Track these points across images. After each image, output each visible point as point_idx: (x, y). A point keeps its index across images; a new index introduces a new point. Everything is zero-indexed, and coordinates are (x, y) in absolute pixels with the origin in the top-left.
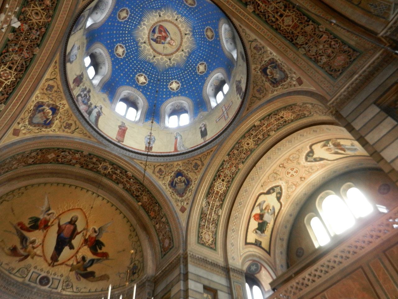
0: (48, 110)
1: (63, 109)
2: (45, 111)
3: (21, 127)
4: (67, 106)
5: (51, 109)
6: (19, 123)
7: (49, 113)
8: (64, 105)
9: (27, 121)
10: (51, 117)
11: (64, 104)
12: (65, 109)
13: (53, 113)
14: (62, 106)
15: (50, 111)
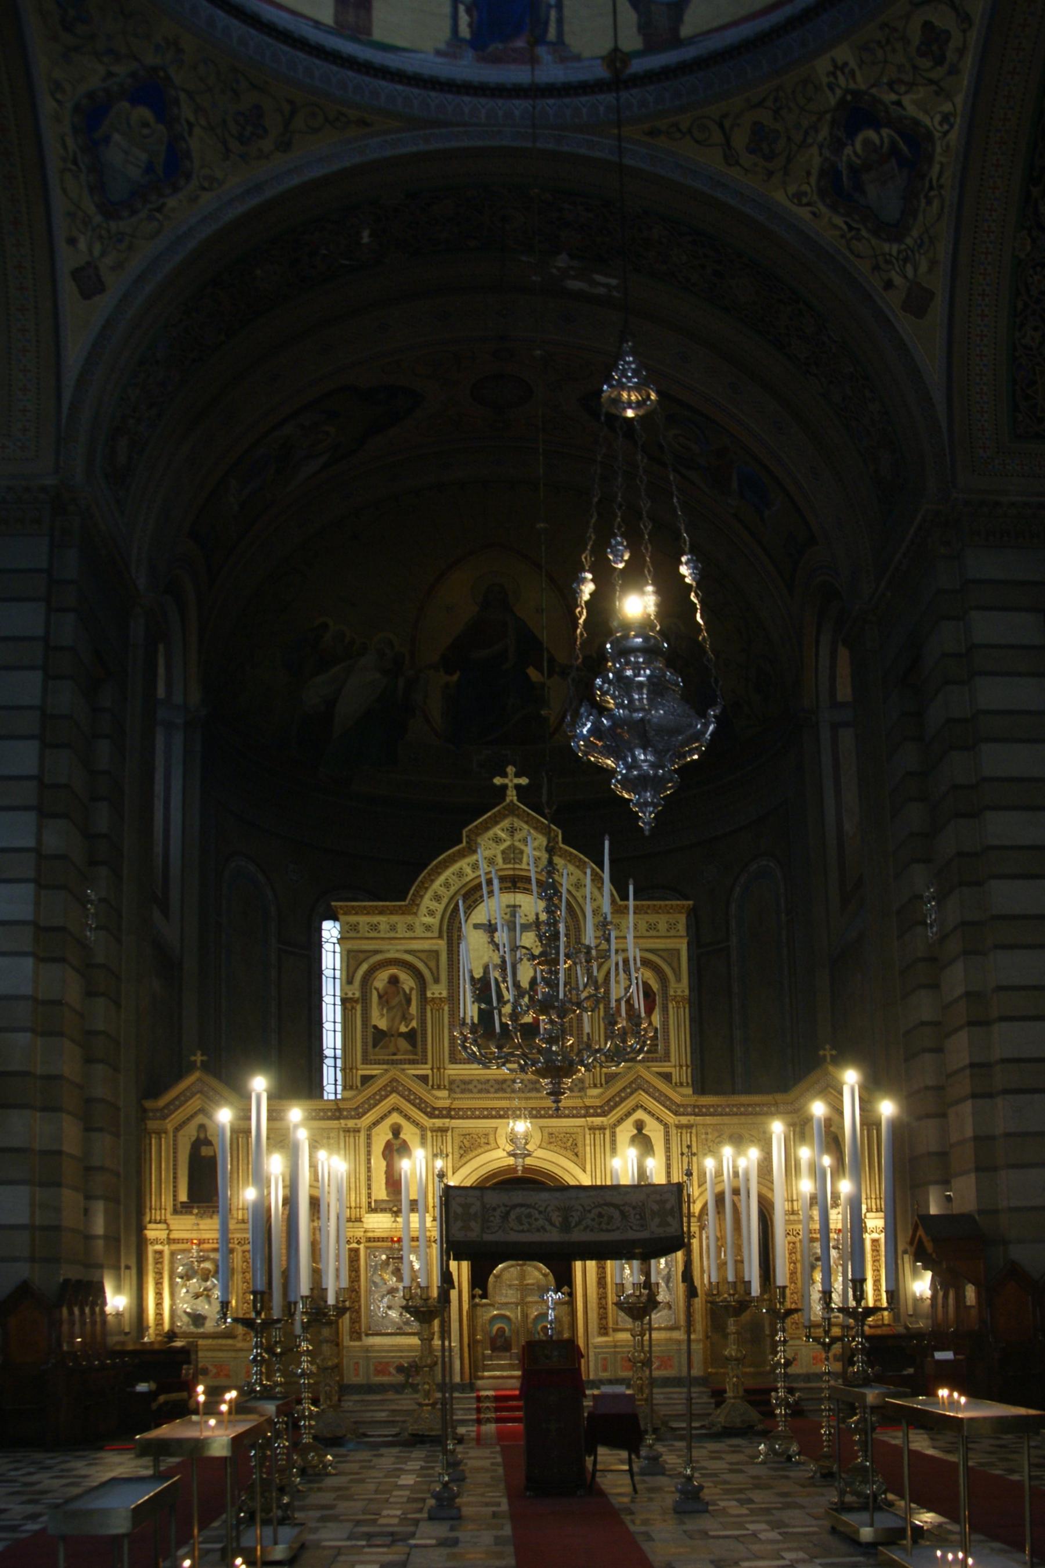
0: (855, 150)
1: (852, 73)
2: (859, 162)
3: (905, 277)
4: (843, 53)
5: (852, 133)
6: (889, 285)
7: (867, 142)
8: (838, 68)
9: (886, 247)
10: (885, 132)
11: (831, 69)
12: (853, 64)
13: (877, 126)
14: (842, 80)
15: (859, 140)
